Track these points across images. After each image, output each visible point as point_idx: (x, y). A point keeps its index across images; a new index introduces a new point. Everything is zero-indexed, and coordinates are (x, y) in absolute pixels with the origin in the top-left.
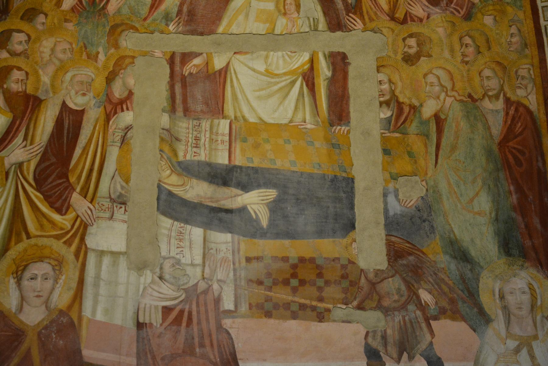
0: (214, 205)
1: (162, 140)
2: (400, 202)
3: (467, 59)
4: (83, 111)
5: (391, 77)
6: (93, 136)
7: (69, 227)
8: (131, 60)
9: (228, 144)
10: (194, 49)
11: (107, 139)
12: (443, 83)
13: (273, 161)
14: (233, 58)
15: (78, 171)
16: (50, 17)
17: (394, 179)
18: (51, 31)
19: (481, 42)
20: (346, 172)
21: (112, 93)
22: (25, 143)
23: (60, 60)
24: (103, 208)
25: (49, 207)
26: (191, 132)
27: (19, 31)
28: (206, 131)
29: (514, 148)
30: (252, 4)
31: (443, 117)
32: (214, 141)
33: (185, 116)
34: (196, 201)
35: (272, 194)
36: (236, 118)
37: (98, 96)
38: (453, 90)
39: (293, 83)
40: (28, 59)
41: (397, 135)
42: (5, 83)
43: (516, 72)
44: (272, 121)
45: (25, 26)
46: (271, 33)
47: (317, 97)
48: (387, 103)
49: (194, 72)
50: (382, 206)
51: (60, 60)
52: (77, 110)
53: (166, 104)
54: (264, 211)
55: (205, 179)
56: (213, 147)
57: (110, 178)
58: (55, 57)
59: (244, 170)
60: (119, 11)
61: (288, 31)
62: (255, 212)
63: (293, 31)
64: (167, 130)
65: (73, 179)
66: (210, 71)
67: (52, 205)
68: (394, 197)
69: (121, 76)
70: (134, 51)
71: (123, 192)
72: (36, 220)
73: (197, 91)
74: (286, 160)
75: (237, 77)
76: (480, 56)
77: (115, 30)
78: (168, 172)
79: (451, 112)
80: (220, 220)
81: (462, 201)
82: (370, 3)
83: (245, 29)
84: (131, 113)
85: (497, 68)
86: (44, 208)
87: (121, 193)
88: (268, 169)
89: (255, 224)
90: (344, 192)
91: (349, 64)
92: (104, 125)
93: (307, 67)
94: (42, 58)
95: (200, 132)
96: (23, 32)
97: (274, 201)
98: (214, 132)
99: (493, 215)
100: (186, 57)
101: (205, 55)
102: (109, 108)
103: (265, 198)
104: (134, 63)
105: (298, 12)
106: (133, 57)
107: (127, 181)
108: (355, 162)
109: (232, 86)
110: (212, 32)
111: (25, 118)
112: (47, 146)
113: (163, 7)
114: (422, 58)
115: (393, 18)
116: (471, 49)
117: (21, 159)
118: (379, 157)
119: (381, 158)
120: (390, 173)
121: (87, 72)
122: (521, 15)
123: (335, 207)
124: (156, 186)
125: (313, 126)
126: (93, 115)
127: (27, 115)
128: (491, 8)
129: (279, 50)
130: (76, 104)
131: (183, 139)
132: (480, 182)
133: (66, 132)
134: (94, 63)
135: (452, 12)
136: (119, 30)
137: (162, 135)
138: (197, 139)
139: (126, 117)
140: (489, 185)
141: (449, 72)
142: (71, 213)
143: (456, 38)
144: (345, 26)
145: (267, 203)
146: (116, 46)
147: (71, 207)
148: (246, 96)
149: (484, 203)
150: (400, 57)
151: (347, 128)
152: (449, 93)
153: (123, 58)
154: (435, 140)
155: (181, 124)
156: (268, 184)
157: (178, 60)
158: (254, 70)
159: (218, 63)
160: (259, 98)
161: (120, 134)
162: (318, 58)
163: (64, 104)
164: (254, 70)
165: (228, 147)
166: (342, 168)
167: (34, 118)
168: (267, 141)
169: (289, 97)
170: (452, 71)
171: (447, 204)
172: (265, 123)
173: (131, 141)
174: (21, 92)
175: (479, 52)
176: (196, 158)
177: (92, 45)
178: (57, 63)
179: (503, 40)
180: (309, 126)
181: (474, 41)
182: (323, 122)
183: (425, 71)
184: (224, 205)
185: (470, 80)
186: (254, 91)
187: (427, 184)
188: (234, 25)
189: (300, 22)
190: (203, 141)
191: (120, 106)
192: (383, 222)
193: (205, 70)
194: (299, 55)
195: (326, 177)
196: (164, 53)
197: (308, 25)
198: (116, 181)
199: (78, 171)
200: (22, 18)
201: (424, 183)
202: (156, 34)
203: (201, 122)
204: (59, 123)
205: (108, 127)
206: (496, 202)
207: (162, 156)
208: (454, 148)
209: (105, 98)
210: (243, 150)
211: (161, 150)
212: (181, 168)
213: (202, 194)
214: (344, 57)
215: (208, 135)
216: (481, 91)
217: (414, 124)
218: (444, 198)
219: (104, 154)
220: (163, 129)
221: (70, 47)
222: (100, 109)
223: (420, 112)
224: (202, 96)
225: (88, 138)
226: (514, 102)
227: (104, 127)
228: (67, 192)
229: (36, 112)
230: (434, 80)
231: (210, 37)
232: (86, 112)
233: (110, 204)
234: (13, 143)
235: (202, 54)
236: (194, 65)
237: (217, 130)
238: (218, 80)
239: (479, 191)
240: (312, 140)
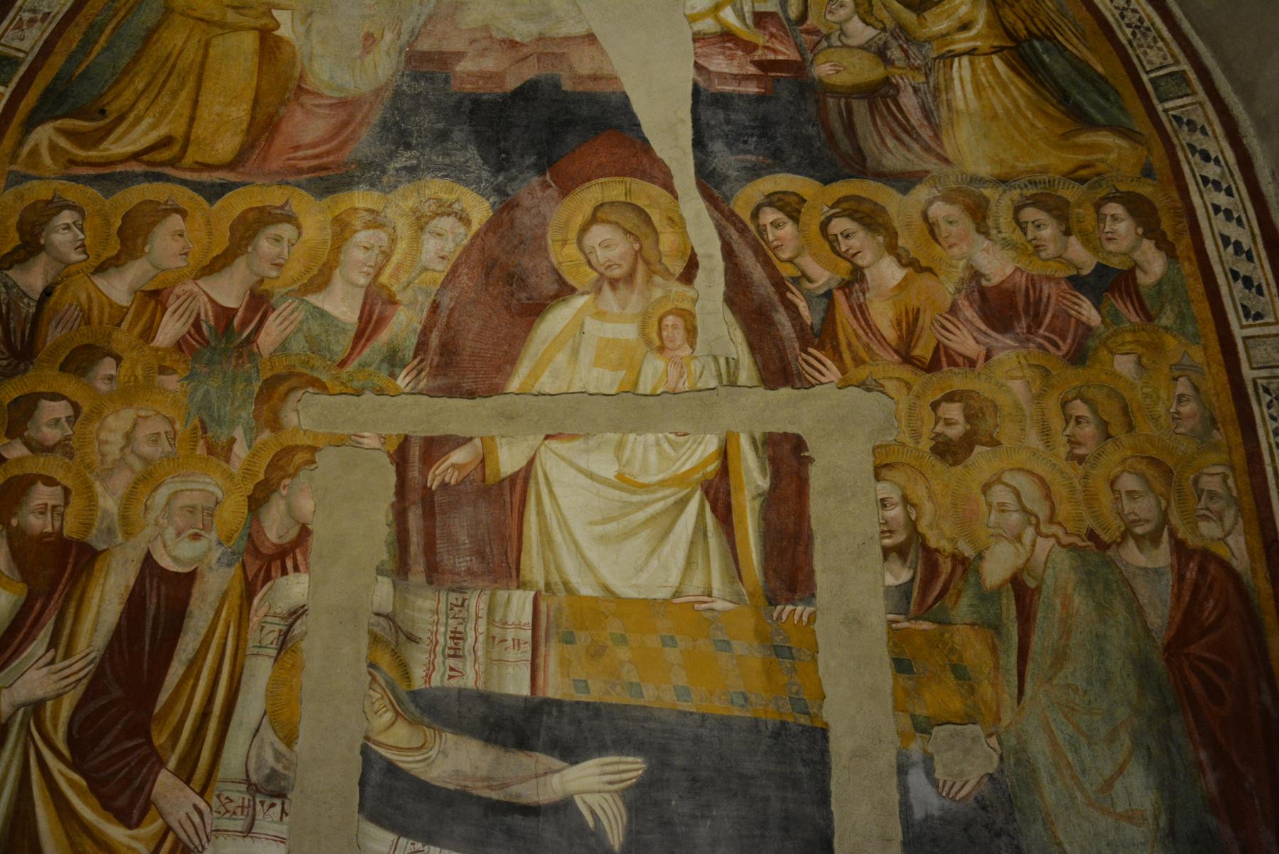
0: (495, 795)
1: (375, 639)
2: (937, 787)
3: (1080, 451)
4: (191, 577)
5: (908, 492)
6: (214, 633)
8: (307, 456)
9: (529, 648)
10: (454, 429)
11: (246, 641)
12: (1029, 506)
13: (635, 688)
14: (543, 448)
15: (174, 719)
16: (126, 364)
17: (923, 732)
18: (127, 394)
19: (1111, 411)
20: (808, 713)
21: (261, 531)
22: (52, 652)
23: (146, 460)
24: (231, 807)
25: (101, 809)
26: (443, 620)
27: (55, 397)
28: (478, 617)
29: (1203, 660)
30: (586, 329)
31: (1032, 584)
32: (497, 640)
33: (430, 582)
34: (451, 787)
35: (632, 767)
36: (548, 586)
37: (229, 539)
38: (1052, 520)
39: (682, 503)
40: (71, 458)
41: (925, 625)
42: (15, 514)
43: (1196, 482)
44: (632, 594)
45: (69, 386)
46: (630, 390)
47: (738, 537)
48: (901, 551)
49: (453, 482)
50: (897, 797)
51: (142, 458)
52: (177, 573)
53: (385, 557)
54: (614, 808)
55: (473, 733)
56: (495, 656)
57: (249, 734)
58: (133, 452)
59: (566, 709)
60: (283, 346)
61: (671, 386)
62: (593, 813)
63: (680, 387)
64: (387, 617)
65: (160, 739)
66: (490, 480)
68: (923, 775)
69: (284, 492)
70: (316, 436)
71: (279, 767)
72: (65, 842)
73: (459, 525)
74: (668, 685)
75: (551, 492)
76: (1109, 445)
77: (275, 389)
78: (389, 716)
79: (1049, 571)
80: (510, 833)
81: (1087, 786)
82: (856, 326)
83: (570, 382)
84: (304, 578)
85: (1151, 472)
86: (87, 812)
87: (273, 771)
88: (624, 709)
89: (592, 841)
90: (805, 763)
91: (810, 460)
92: (241, 607)
93: (713, 467)
94: (103, 455)
95: (464, 621)
96: (63, 398)
97: (638, 785)
98: (497, 619)
99: (1163, 821)
100: (435, 447)
101: (477, 442)
103: (617, 777)
104: (314, 462)
105: (692, 346)
106: (314, 449)
107: (290, 739)
108: (828, 689)
109: (541, 513)
110: (495, 390)
111: (56, 596)
113: (384, 336)
114: (978, 449)
115: (907, 358)
116: (1089, 430)
117: (40, 693)
118: (885, 676)
119: (891, 681)
120: (913, 717)
121: (205, 484)
122: (1197, 355)
123: (784, 800)
124: (357, 751)
125: (729, 605)
126: (217, 582)
127: (61, 587)
128: (1129, 337)
129: (648, 430)
130: (176, 560)
131: (425, 636)
132: (1125, 741)
133: (149, 625)
134: (223, 463)
135: (1040, 346)
136: (282, 388)
137: (376, 629)
138: (457, 637)
139: (294, 588)
140: (1149, 748)
141: (1042, 480)
142: (154, 820)
143: (1052, 403)
144: (800, 376)
145: (623, 790)
146: (275, 424)
147: (153, 807)
148: (571, 535)
149: (1138, 790)
150: (926, 444)
151: (810, 609)
152: (1043, 529)
153: (289, 451)
154: (1015, 638)
155: (419, 602)
156: (623, 744)
157: (415, 453)
158: (590, 476)
159: (509, 460)
160: (603, 539)
161: (277, 628)
162: (739, 448)
163: (148, 559)
164: (590, 476)
165: (529, 656)
166: (799, 705)
167: (76, 595)
168: (622, 640)
169: (673, 536)
170: (1048, 478)
171: (1050, 794)
172: (617, 598)
173: (303, 644)
174: (49, 535)
175: (1109, 436)
176: (454, 683)
177: (219, 425)
178: (138, 465)
179: (1161, 409)
180: (719, 605)
181: (1095, 412)
182: (751, 595)
183: (986, 477)
184: (519, 796)
185: (1091, 499)
186: (591, 523)
187: (1000, 743)
188: (547, 373)
189: (696, 366)
190: (470, 641)
191: (279, 563)
192: (900, 837)
193: (478, 477)
194: (695, 441)
195: (762, 727)
196: (384, 439)
197: (715, 374)
199: (174, 719)
200: (63, 368)
201: (993, 741)
202: (368, 396)
203: (467, 596)
204: (135, 603)
205: (249, 610)
206: (1167, 788)
207: (374, 679)
208: (1060, 658)
209: (243, 543)
210: (564, 664)
211: (372, 665)
212: (417, 706)
213: (466, 768)
214: (798, 444)
215: (482, 628)
216: (1116, 525)
217: (965, 601)
218: (1044, 777)
219: (236, 676)
220: (378, 614)
221: (169, 429)
222: (233, 570)
223: (977, 572)
224: (470, 536)
225: (201, 639)
226: (1195, 551)
227: (241, 613)
228: (145, 770)
229: (83, 579)
230: (1009, 499)
231: (488, 402)
232: (199, 577)
233: (247, 797)
234: (25, 654)
235: (471, 439)
236: (453, 466)
237: (505, 616)
238: (508, 499)
239: (1126, 762)
240: (727, 638)
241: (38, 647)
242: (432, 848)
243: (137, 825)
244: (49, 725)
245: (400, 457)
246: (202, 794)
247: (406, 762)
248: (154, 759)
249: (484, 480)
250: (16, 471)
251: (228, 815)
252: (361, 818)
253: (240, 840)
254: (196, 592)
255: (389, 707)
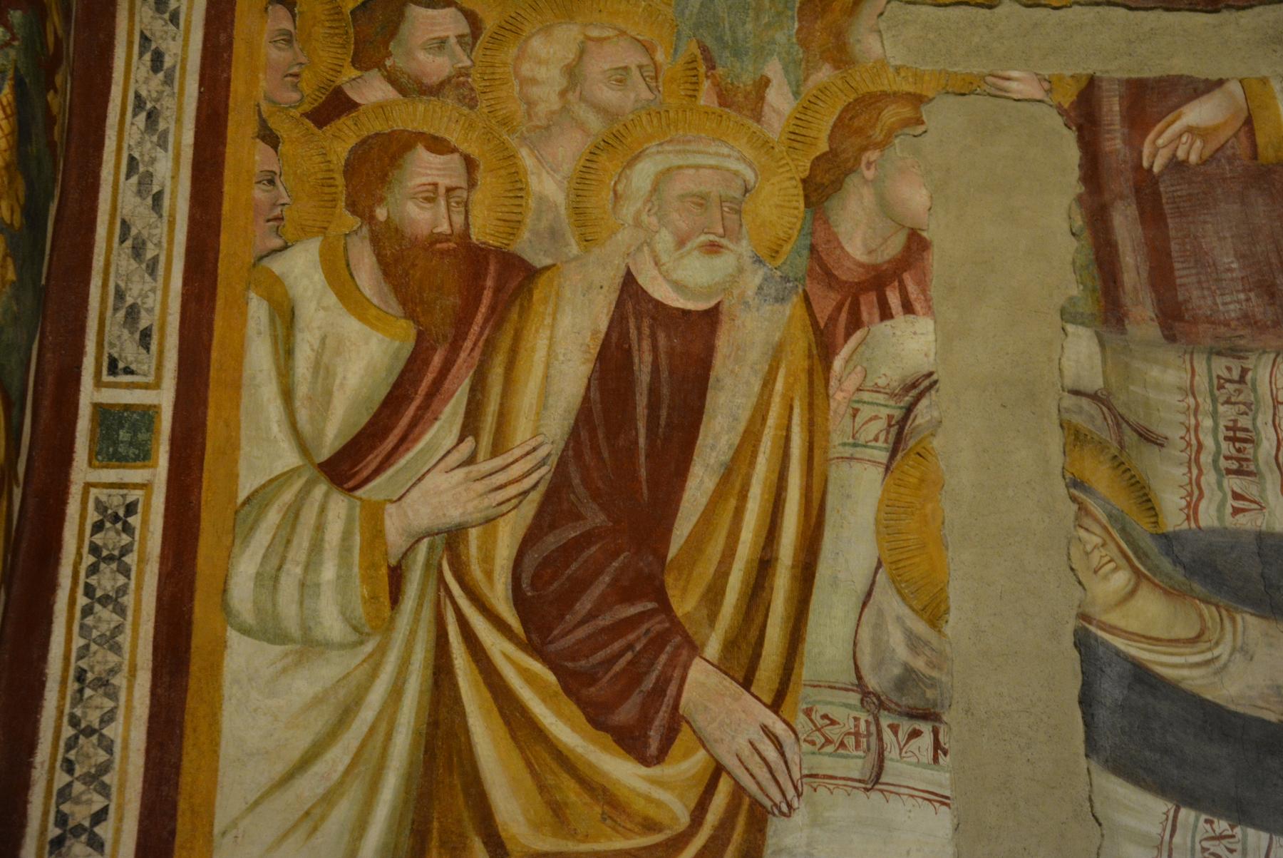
1: (1076, 437)
4: (711, 317)
6: (764, 419)
7: (685, 820)
10: (1181, 65)
11: (827, 433)
21: (833, 240)
22: (469, 443)
24: (834, 733)
25: (589, 727)
26: (1206, 405)
37: (775, 253)
40: (472, 108)
42: (381, 200)
49: (1193, 158)
52: (685, 313)
53: (1075, 291)
57: (855, 603)
58: (582, 98)
64: (1094, 397)
65: (685, 604)
67: (596, 716)
69: (869, 174)
70: (918, 76)
71: (919, 664)
72: (529, 782)
78: (1121, 579)
86: (565, 729)
87: (909, 670)
92: (810, 372)
94: (530, 104)
95: (1250, 408)
101: (1234, 87)
102: (825, 304)
104: (919, 121)
106: (918, 100)
107: (934, 614)
111: (468, 344)
112: (562, 462)
117: (454, 515)
121: (720, 159)
124: (1069, 640)
127: (475, 328)
130: (679, 287)
131: (1175, 434)
133: (642, 401)
134: (750, 122)
137: (1077, 420)
138: (1240, 437)
139: (907, 343)
142: (686, 755)
146: (841, 56)
147: (685, 727)
153: (870, 102)
155: (1155, 372)
157: (1112, 108)
161: (884, 412)
167: (505, 342)
173: (936, 443)
174: (446, 238)
176: (1244, 521)
177: (737, 53)
178: (595, 123)
191: (873, 296)
193: (1242, 148)
196: (1050, 84)
198: (880, 613)
203: (1249, 364)
204: (612, 361)
205: (827, 381)
207: (1082, 508)
209: (803, 262)
211: (1076, 483)
212: (1176, 561)
219: (816, 496)
220: (1076, 393)
221: (645, 60)
222: (788, 309)
224: (1241, 257)
225: (741, 427)
227: (811, 383)
228: (663, 658)
229: (514, 316)
232: (724, 318)
233: (863, 717)
234: (420, 445)
235: (1221, 83)
236: (1190, 130)
241: (444, 429)
242: (1251, 832)
243: (660, 758)
244: (476, 571)
245: (1084, 112)
246: (776, 706)
247: (1166, 664)
248: (678, 639)
249: (1255, 156)
250: (379, 126)
251: (830, 749)
252: (1094, 766)
253: (861, 795)
254: (723, 344)
255: (1123, 562)
